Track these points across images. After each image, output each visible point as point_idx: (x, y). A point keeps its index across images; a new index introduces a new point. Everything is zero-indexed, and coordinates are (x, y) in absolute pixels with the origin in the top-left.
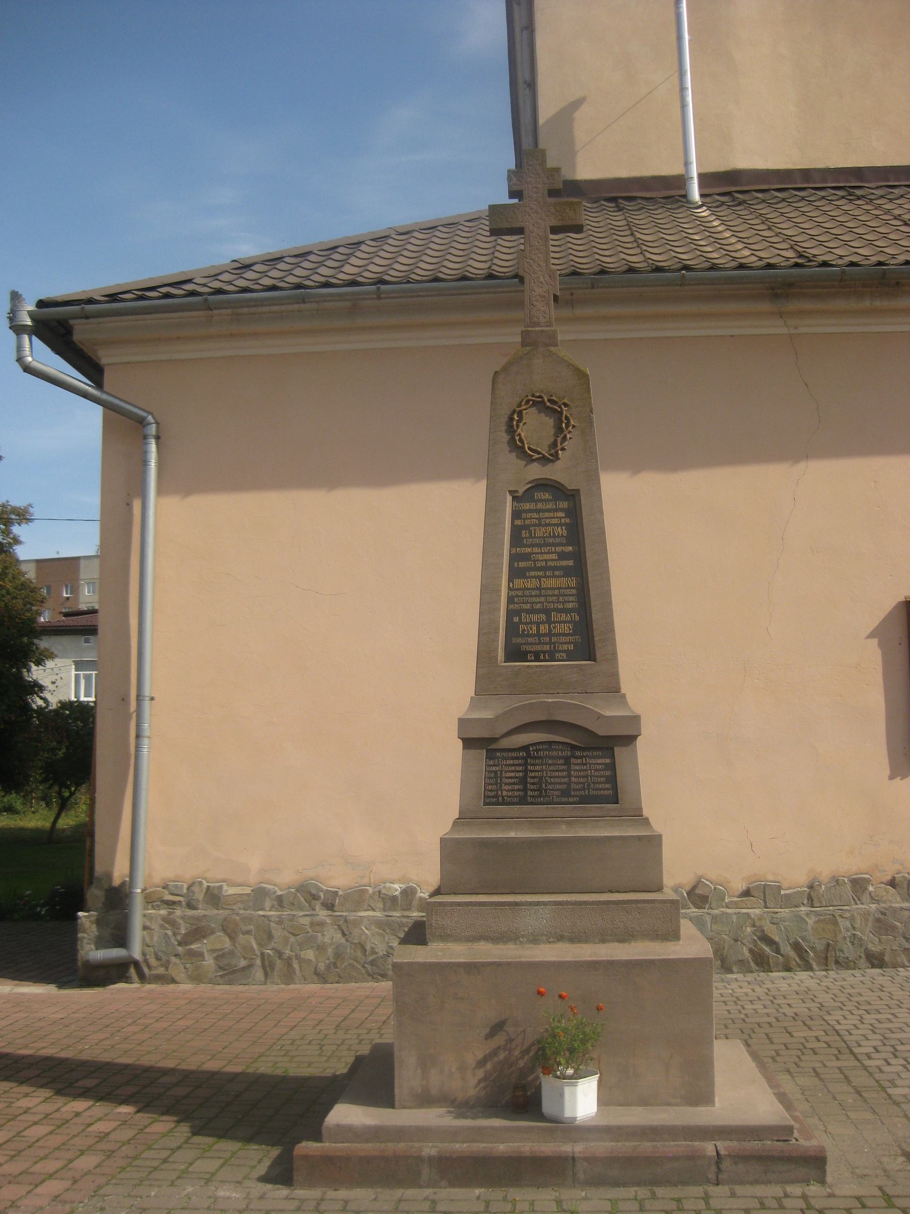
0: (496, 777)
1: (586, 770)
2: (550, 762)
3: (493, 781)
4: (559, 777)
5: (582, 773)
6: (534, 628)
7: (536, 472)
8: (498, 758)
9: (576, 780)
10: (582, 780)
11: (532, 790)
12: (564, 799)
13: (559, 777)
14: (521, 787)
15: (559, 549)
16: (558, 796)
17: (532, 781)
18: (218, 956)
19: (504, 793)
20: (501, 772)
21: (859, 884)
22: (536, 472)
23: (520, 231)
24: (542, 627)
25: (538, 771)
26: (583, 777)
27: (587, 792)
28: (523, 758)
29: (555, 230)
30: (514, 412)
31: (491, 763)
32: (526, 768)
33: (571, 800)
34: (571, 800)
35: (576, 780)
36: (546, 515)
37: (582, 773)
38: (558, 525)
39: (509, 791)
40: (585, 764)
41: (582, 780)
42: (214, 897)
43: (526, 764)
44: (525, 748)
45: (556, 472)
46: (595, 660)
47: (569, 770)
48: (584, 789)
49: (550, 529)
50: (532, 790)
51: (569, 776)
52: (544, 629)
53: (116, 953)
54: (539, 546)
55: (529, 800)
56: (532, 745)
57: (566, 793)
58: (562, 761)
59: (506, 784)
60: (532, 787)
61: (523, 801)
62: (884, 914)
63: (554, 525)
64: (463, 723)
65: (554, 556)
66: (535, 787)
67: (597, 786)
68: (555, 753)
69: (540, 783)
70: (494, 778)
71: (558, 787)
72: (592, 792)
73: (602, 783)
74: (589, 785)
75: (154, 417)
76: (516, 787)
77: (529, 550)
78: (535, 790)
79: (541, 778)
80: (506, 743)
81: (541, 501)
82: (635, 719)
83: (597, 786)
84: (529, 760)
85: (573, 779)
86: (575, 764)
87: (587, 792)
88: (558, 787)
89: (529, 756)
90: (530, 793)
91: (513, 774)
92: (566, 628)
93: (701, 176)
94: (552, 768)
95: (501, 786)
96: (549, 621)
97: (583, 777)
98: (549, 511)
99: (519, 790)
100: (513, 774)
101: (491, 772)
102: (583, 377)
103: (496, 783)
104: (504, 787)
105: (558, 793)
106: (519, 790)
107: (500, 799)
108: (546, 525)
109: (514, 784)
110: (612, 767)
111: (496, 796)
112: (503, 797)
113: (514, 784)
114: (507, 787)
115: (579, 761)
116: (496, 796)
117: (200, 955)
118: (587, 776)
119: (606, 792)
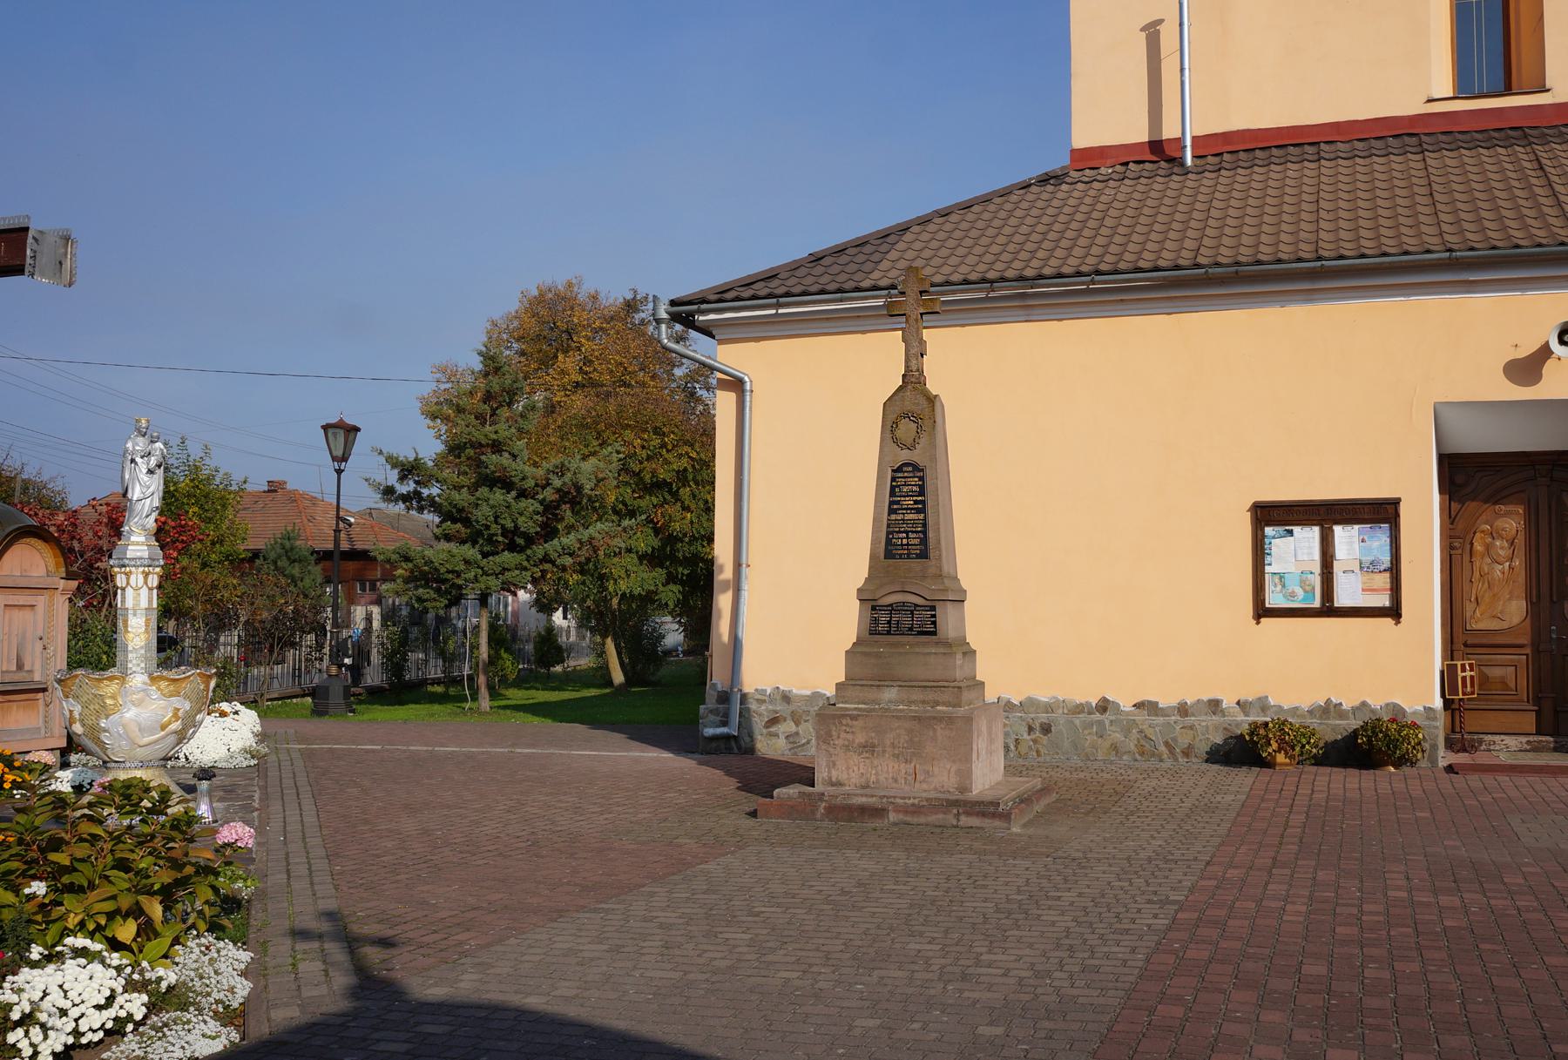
21: (1215, 705)
22: (904, 456)
42: (786, 698)
45: (916, 456)
53: (724, 730)
57: (911, 629)
61: (889, 633)
70: (875, 621)
80: (881, 602)
92: (917, 541)
93: (1194, 138)
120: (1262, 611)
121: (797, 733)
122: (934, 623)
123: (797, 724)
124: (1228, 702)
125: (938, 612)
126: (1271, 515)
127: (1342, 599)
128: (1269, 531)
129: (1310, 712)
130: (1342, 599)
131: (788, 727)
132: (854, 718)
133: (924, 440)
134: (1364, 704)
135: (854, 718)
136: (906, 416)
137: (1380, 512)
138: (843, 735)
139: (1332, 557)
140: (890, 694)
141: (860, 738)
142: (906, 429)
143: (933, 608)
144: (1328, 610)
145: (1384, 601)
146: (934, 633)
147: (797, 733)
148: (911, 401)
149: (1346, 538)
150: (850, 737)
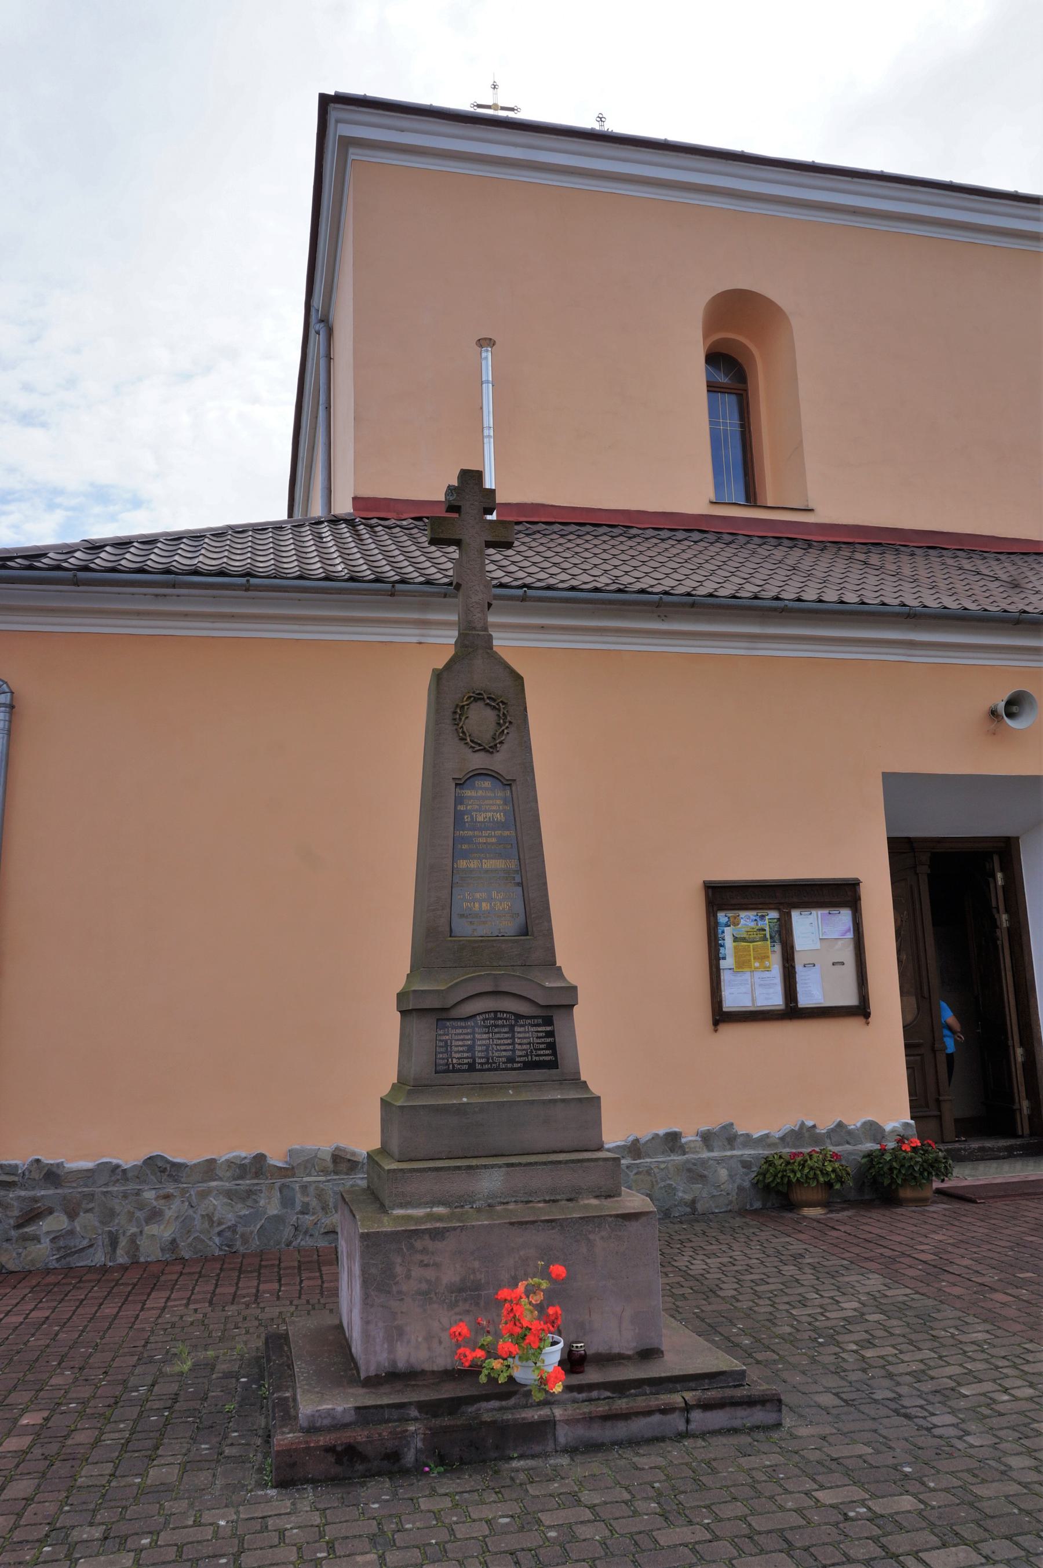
2: (496, 1030)
3: (442, 1050)
5: (525, 1041)
6: (477, 905)
7: (478, 761)
10: (524, 1047)
11: (480, 1058)
12: (510, 1066)
14: (469, 1055)
15: (498, 833)
17: (480, 1048)
18: (54, 1238)
19: (455, 1061)
23: (458, 543)
24: (484, 904)
29: (489, 545)
30: (457, 706)
31: (441, 1032)
33: (516, 1065)
34: (516, 1065)
35: (519, 1047)
36: (487, 802)
37: (525, 1041)
38: (496, 811)
39: (459, 1058)
41: (524, 1047)
42: (52, 1176)
46: (532, 935)
47: (513, 1038)
48: (527, 1055)
49: (489, 814)
50: (480, 1058)
51: (513, 1044)
52: (485, 906)
54: (481, 830)
55: (478, 1067)
57: (511, 1060)
58: (506, 1030)
60: (480, 1055)
62: (695, 1164)
63: (494, 811)
64: (401, 996)
65: (494, 840)
66: (483, 1054)
67: (539, 1052)
68: (500, 1022)
69: (487, 1050)
71: (504, 1053)
72: (534, 1058)
75: (8, 686)
76: (465, 1055)
77: (470, 833)
79: (487, 1046)
81: (481, 788)
82: (574, 989)
83: (539, 1052)
88: (504, 1053)
91: (460, 1043)
94: (498, 1036)
96: (490, 899)
98: (490, 798)
100: (460, 1043)
102: (518, 679)
103: (446, 1052)
105: (504, 1060)
108: (486, 811)
109: (463, 1052)
110: (551, 1034)
111: (447, 1064)
113: (463, 1052)
115: (522, 1029)
116: (447, 1064)
117: (36, 1239)
118: (529, 1043)
119: (547, 1058)
120: (721, 1017)
121: (71, 1232)
122: (552, 1046)
123: (72, 1215)
124: (689, 1137)
125: (559, 1024)
126: (722, 897)
127: (809, 996)
128: (722, 917)
129: (782, 1139)
130: (809, 996)
131: (56, 1222)
132: (437, 1234)
133: (511, 740)
134: (840, 1125)
135: (437, 1234)
136: (478, 698)
137: (842, 894)
138: (417, 1272)
139: (792, 947)
140: (491, 1182)
141: (451, 1275)
142: (481, 720)
143: (548, 1021)
144: (792, 1011)
145: (850, 999)
146: (553, 1065)
147: (71, 1232)
148: (480, 676)
149: (809, 928)
150: (430, 1274)
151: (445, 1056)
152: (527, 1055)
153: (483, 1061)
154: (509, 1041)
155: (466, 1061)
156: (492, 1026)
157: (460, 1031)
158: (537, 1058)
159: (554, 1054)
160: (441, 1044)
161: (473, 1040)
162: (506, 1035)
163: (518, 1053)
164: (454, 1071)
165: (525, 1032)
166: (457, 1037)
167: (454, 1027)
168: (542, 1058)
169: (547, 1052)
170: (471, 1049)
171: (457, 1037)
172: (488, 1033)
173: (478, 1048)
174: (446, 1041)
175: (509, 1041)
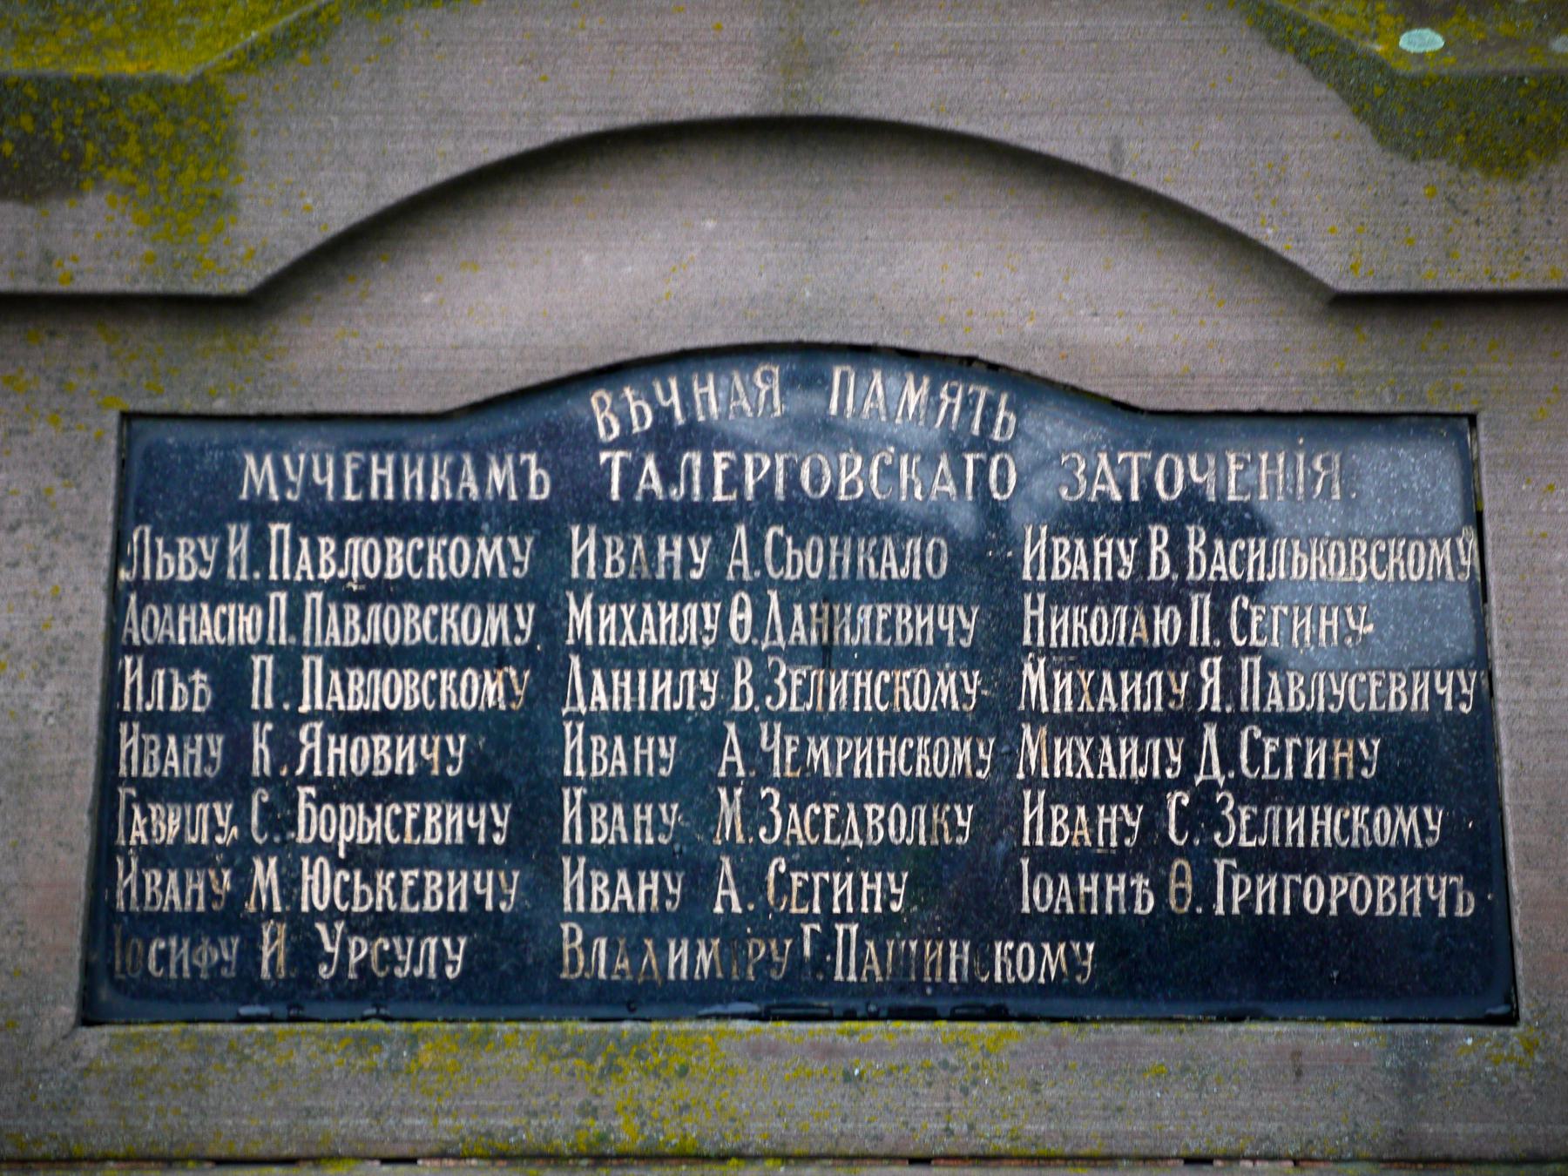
0: (230, 710)
1: (1182, 656)
2: (806, 562)
4: (894, 724)
5: (1135, 691)
8: (260, 513)
9: (1070, 758)
10: (1125, 759)
11: (608, 859)
13: (894, 724)
16: (877, 926)
19: (320, 886)
20: (289, 661)
25: (675, 659)
26: (1139, 725)
27: (1181, 879)
28: (514, 517)
31: (182, 562)
32: (551, 624)
33: (1019, 962)
35: (1070, 758)
37: (1135, 691)
39: (365, 859)
40: (1176, 594)
41: (1125, 759)
43: (544, 588)
44: (536, 409)
47: (999, 651)
48: (1148, 854)
50: (608, 859)
51: (999, 715)
56: (612, 374)
57: (966, 889)
59: (335, 791)
61: (509, 970)
66: (642, 825)
69: (693, 783)
72: (1235, 892)
73: (1336, 791)
74: (1202, 816)
76: (445, 822)
78: (635, 860)
79: (698, 734)
84: (583, 544)
85: (1031, 742)
86: (1061, 594)
87: (1181, 879)
89: (580, 498)
90: (586, 890)
91: (404, 689)
95: (280, 819)
97: (1139, 725)
99: (470, 853)
100: (404, 689)
101: (188, 658)
103: (232, 781)
104: (314, 821)
105: (883, 890)
106: (470, 853)
107: (273, 946)
111: (231, 918)
112: (301, 925)
114: (358, 826)
118: (1182, 722)
119: (1387, 896)
151: (212, 822)
152: (1148, 854)
153: (645, 892)
154: (948, 689)
155: (446, 890)
156: (764, 510)
157: (397, 557)
158: (1267, 893)
159: (1477, 850)
160: (191, 693)
161: (544, 658)
162: (917, 623)
163: (1045, 824)
164: (302, 993)
165: (1140, 593)
166: (351, 628)
167: (322, 518)
168: (1320, 895)
169: (1396, 825)
170: (510, 763)
171: (351, 628)
172: (715, 587)
173: (586, 756)
174: (227, 666)
175: (948, 689)
